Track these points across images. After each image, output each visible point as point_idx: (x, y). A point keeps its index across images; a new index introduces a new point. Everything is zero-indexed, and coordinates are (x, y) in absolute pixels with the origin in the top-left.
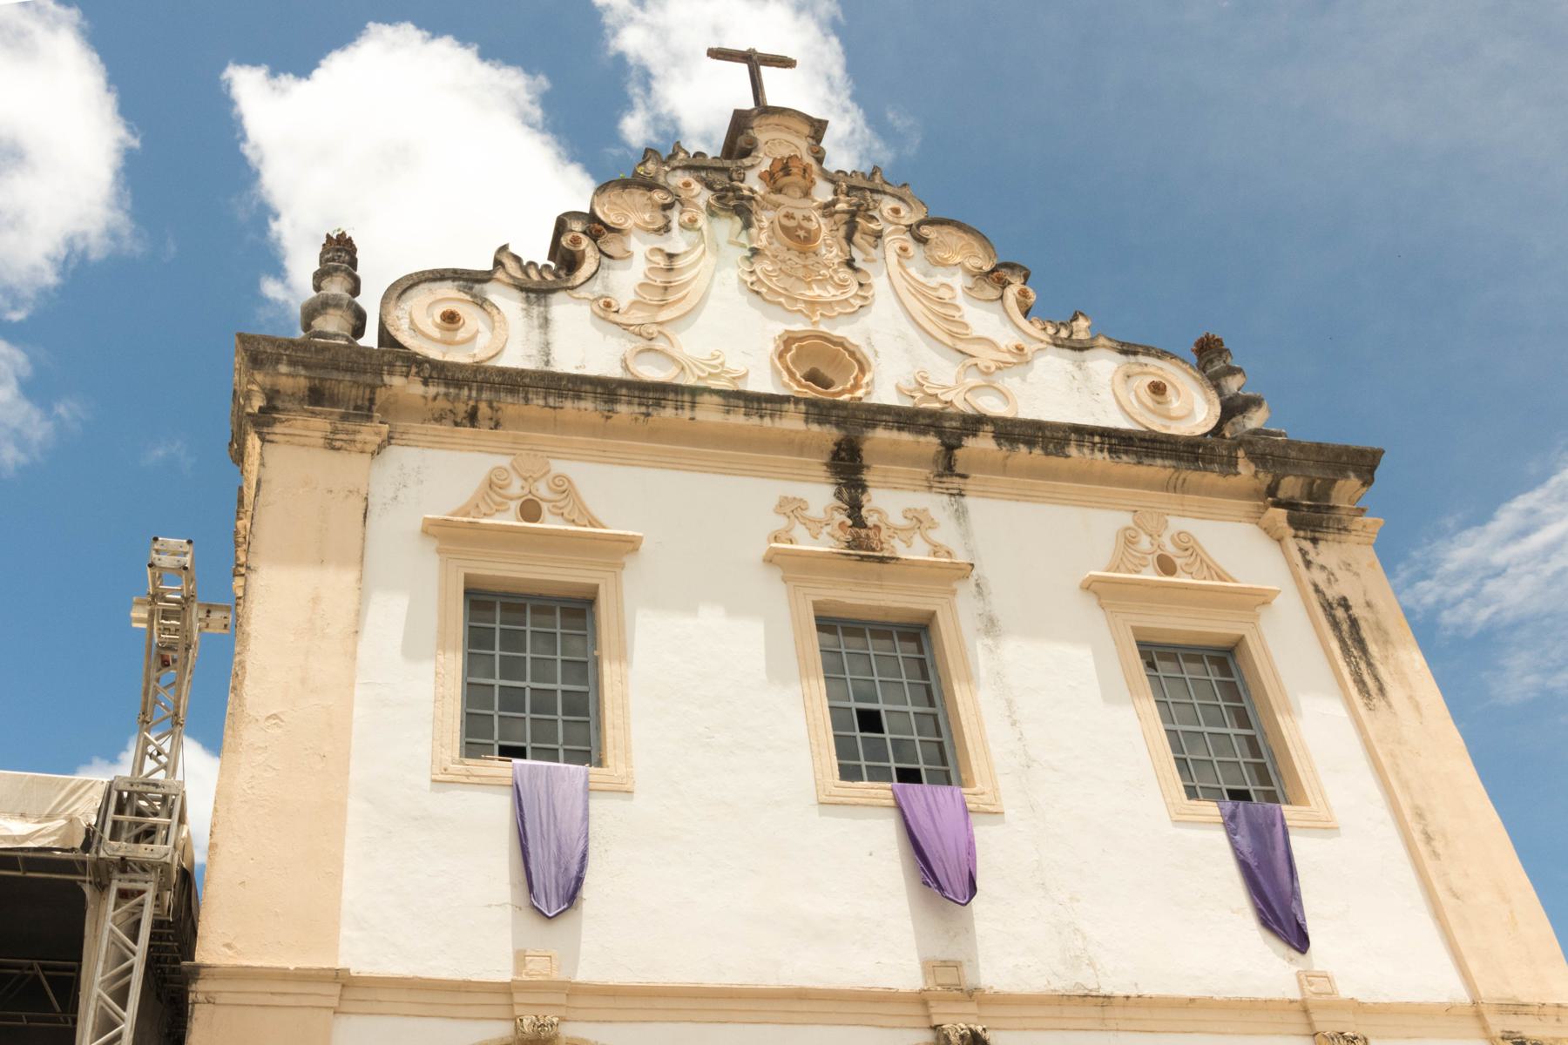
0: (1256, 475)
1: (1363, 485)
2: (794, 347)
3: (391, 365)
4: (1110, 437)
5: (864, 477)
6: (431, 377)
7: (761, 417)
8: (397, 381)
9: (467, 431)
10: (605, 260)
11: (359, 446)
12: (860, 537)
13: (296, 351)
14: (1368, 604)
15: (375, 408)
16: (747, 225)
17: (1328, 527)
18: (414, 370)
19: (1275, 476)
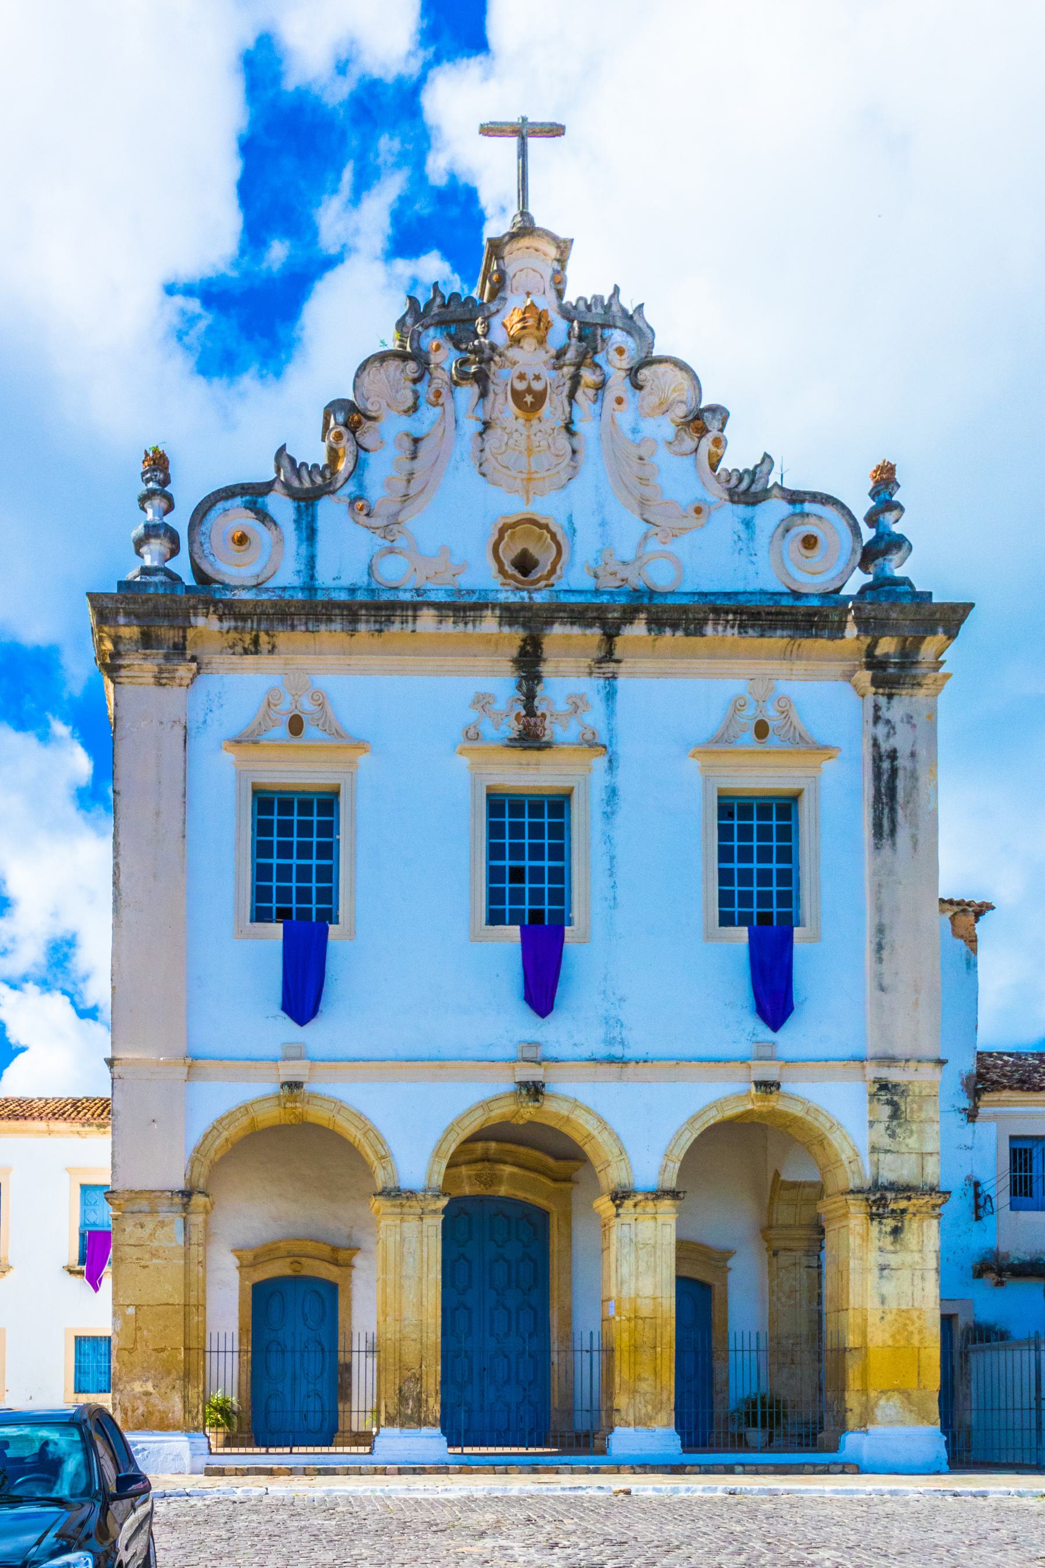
0: (858, 638)
1: (949, 638)
2: (506, 535)
3: (195, 608)
4: (741, 614)
5: (540, 669)
6: (224, 614)
7: (466, 623)
8: (200, 622)
9: (250, 659)
10: (362, 453)
11: (178, 681)
12: (530, 725)
13: (128, 604)
14: (913, 755)
15: (187, 643)
16: (483, 395)
17: (904, 684)
18: (212, 609)
19: (873, 637)
